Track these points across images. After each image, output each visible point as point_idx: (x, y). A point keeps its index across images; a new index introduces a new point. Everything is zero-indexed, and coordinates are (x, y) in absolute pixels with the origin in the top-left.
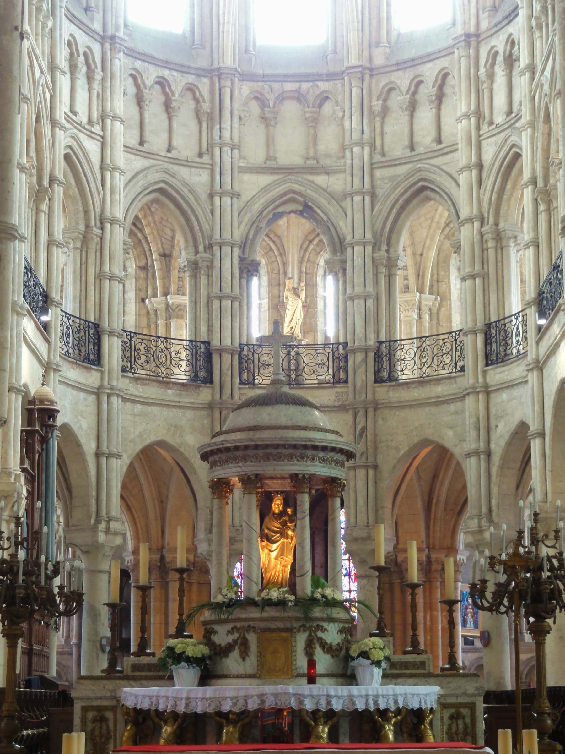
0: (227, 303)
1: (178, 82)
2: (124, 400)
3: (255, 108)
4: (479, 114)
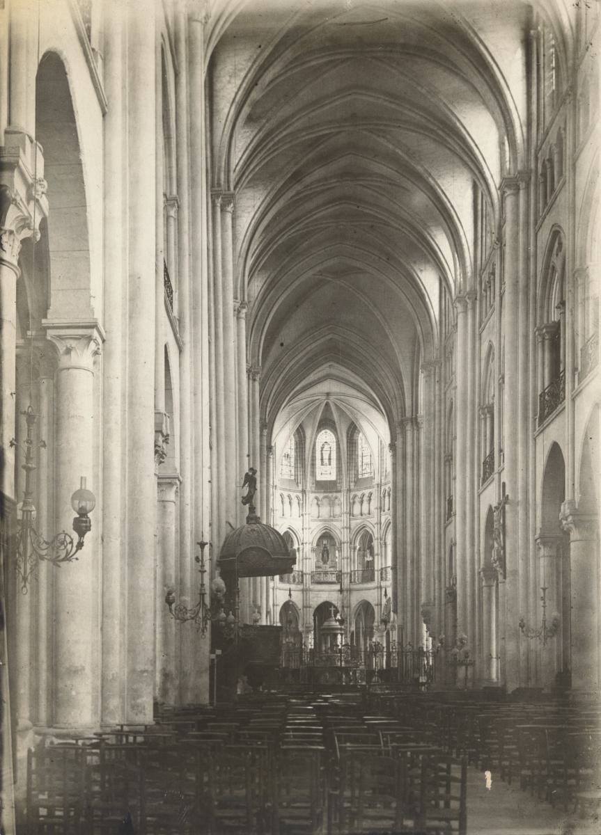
0: (308, 560)
1: (293, 495)
2: (280, 589)
3: (315, 501)
4: (381, 508)
